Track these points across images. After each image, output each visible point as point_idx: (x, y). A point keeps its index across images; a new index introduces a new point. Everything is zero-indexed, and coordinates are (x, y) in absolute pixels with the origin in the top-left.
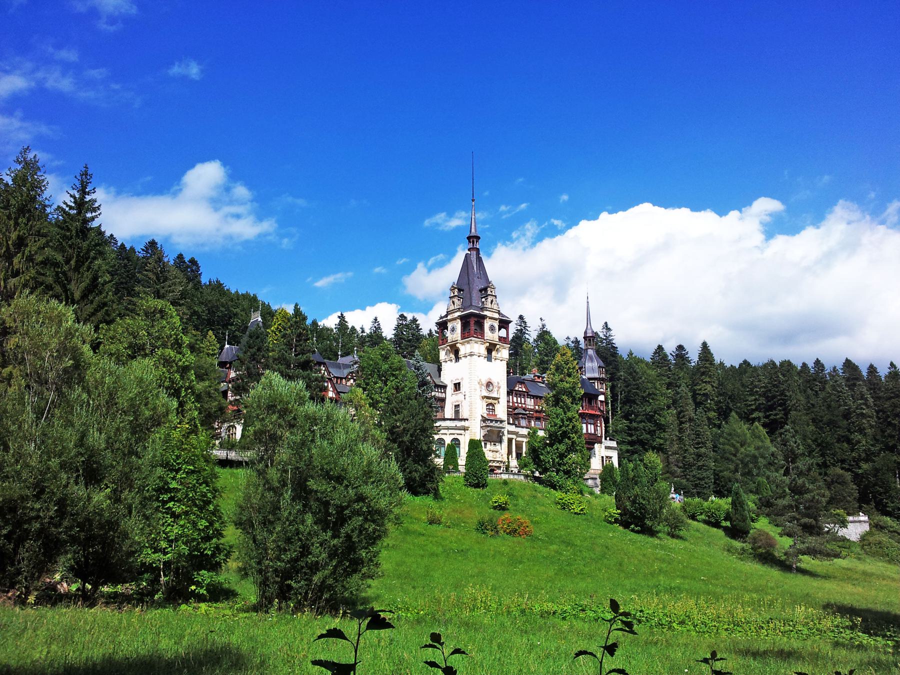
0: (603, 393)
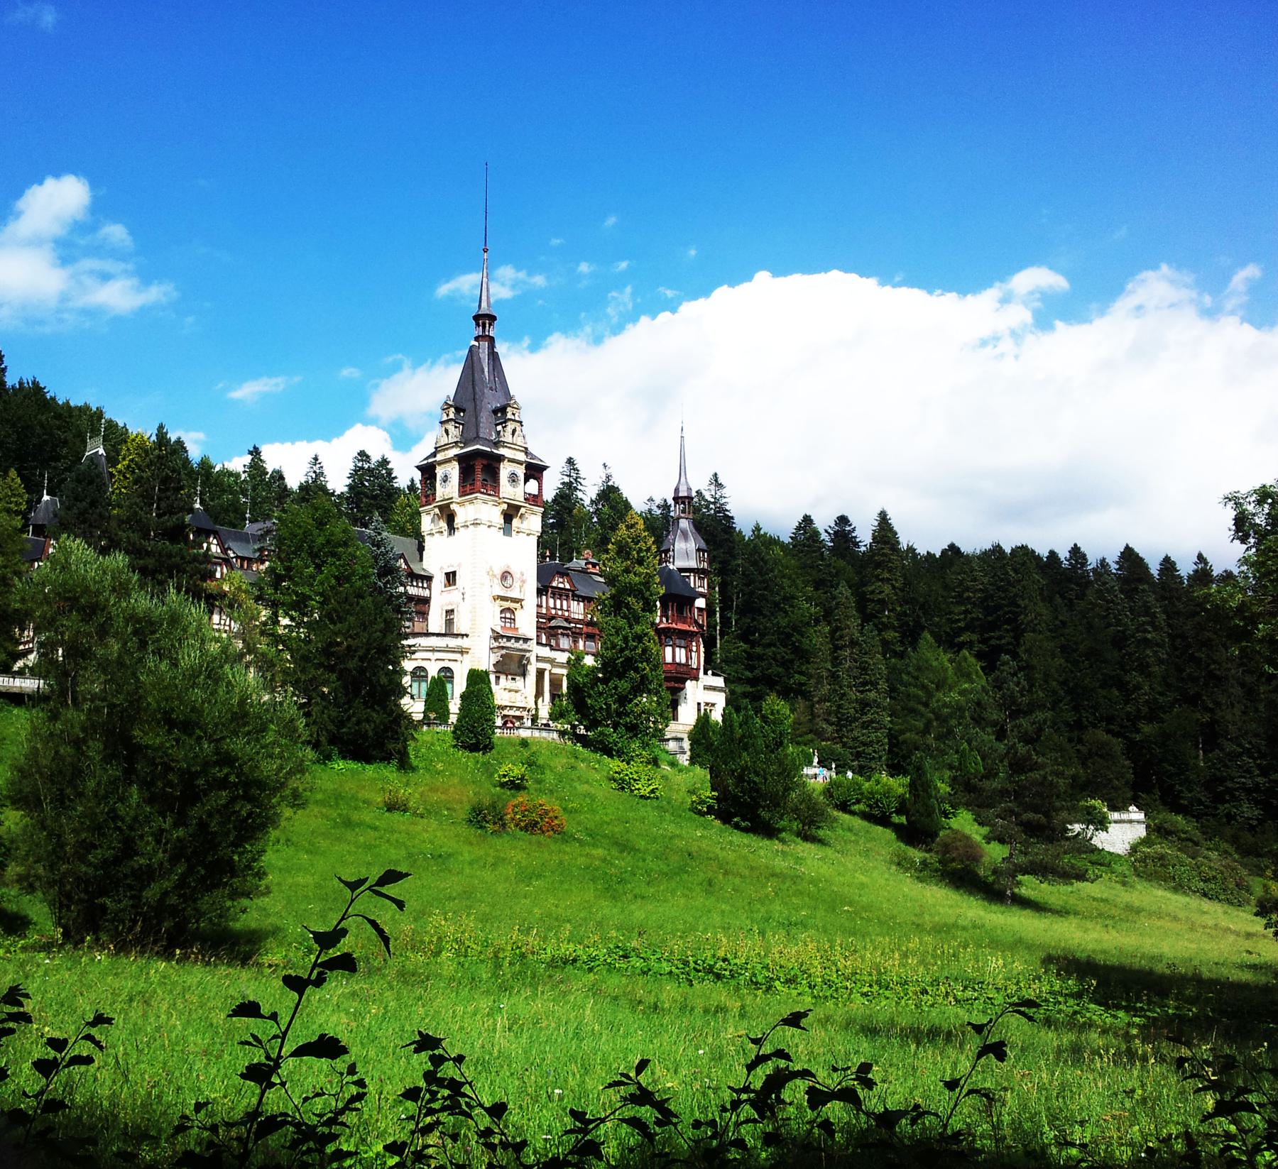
0: (702, 595)
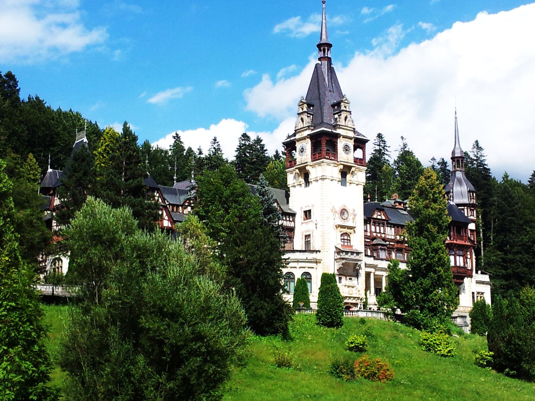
0: (473, 221)
